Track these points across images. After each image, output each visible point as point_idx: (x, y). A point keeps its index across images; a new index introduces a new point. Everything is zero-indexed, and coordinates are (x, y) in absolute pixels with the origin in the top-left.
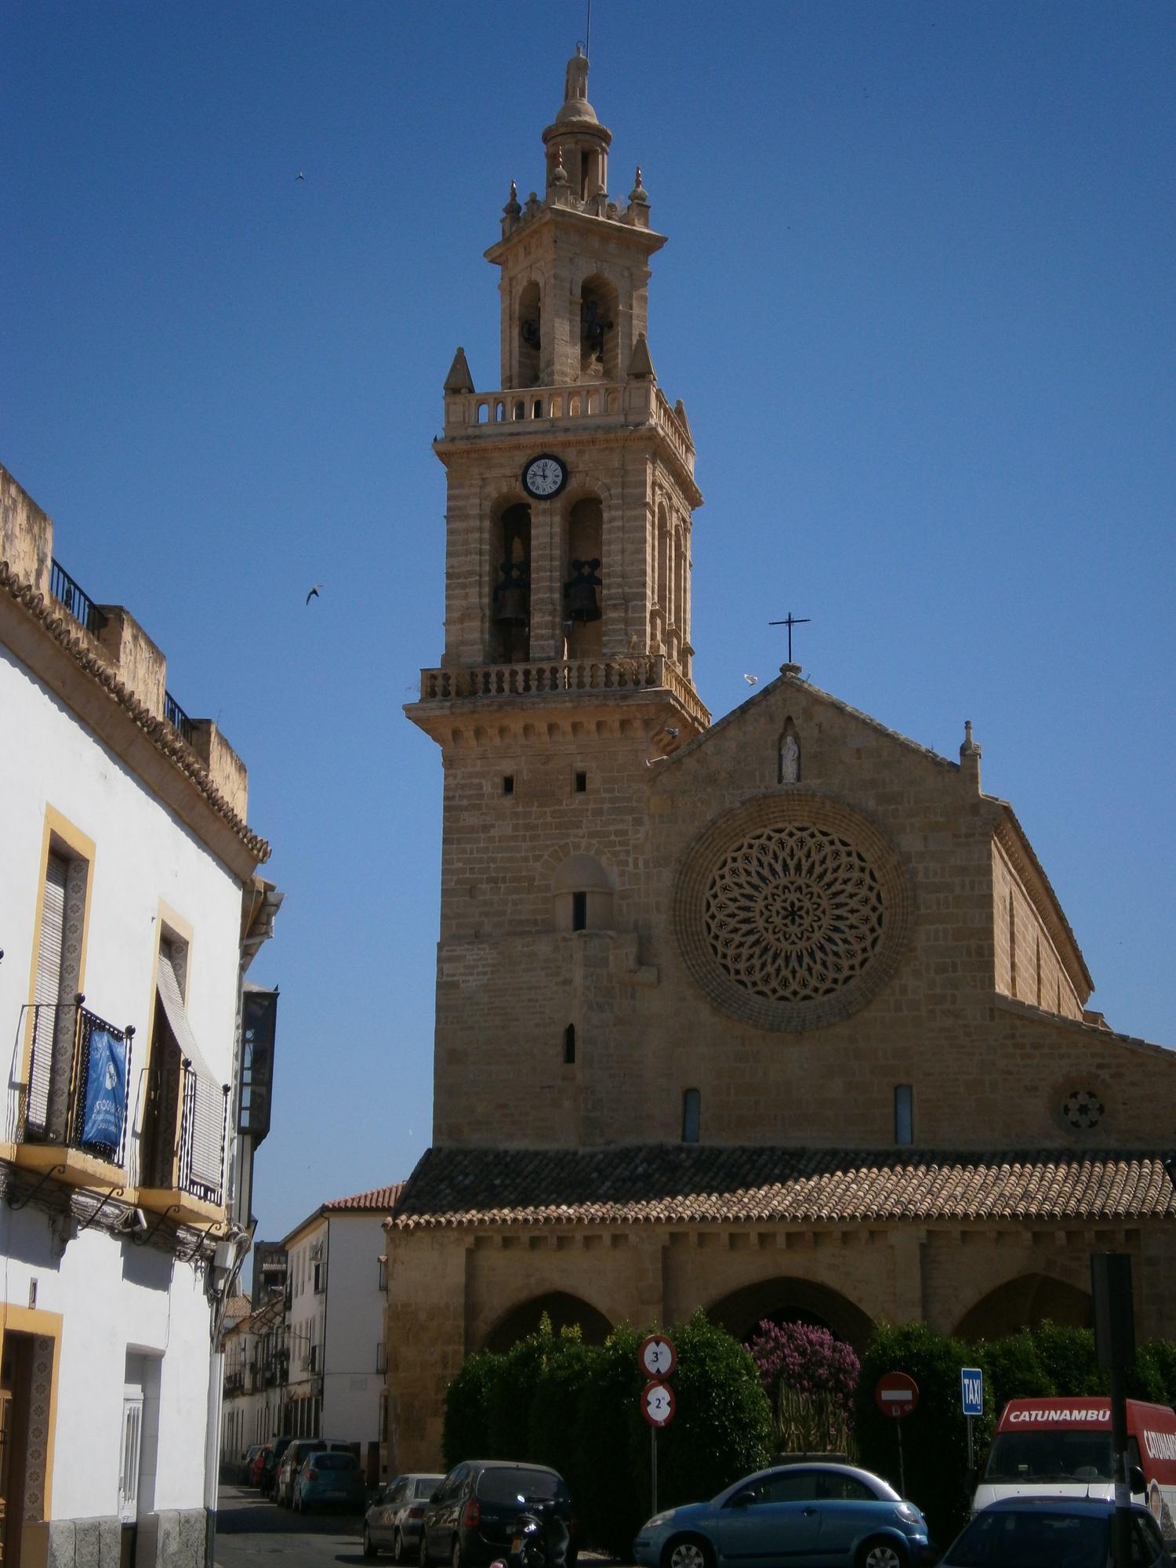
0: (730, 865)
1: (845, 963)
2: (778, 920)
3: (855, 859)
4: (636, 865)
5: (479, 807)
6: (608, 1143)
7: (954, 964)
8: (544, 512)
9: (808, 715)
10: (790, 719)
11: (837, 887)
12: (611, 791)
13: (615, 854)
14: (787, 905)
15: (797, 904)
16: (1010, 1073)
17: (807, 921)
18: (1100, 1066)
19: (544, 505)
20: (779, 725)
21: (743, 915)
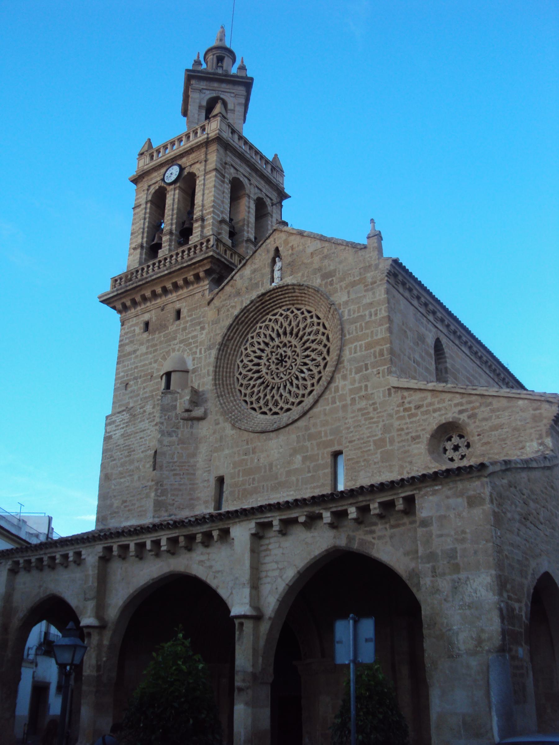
1: (309, 383)
2: (273, 367)
3: (315, 320)
5: (132, 342)
6: (170, 515)
8: (171, 190)
9: (286, 242)
10: (277, 250)
12: (191, 315)
13: (190, 350)
14: (278, 356)
16: (402, 429)
18: (461, 412)
20: (272, 254)
21: (255, 368)
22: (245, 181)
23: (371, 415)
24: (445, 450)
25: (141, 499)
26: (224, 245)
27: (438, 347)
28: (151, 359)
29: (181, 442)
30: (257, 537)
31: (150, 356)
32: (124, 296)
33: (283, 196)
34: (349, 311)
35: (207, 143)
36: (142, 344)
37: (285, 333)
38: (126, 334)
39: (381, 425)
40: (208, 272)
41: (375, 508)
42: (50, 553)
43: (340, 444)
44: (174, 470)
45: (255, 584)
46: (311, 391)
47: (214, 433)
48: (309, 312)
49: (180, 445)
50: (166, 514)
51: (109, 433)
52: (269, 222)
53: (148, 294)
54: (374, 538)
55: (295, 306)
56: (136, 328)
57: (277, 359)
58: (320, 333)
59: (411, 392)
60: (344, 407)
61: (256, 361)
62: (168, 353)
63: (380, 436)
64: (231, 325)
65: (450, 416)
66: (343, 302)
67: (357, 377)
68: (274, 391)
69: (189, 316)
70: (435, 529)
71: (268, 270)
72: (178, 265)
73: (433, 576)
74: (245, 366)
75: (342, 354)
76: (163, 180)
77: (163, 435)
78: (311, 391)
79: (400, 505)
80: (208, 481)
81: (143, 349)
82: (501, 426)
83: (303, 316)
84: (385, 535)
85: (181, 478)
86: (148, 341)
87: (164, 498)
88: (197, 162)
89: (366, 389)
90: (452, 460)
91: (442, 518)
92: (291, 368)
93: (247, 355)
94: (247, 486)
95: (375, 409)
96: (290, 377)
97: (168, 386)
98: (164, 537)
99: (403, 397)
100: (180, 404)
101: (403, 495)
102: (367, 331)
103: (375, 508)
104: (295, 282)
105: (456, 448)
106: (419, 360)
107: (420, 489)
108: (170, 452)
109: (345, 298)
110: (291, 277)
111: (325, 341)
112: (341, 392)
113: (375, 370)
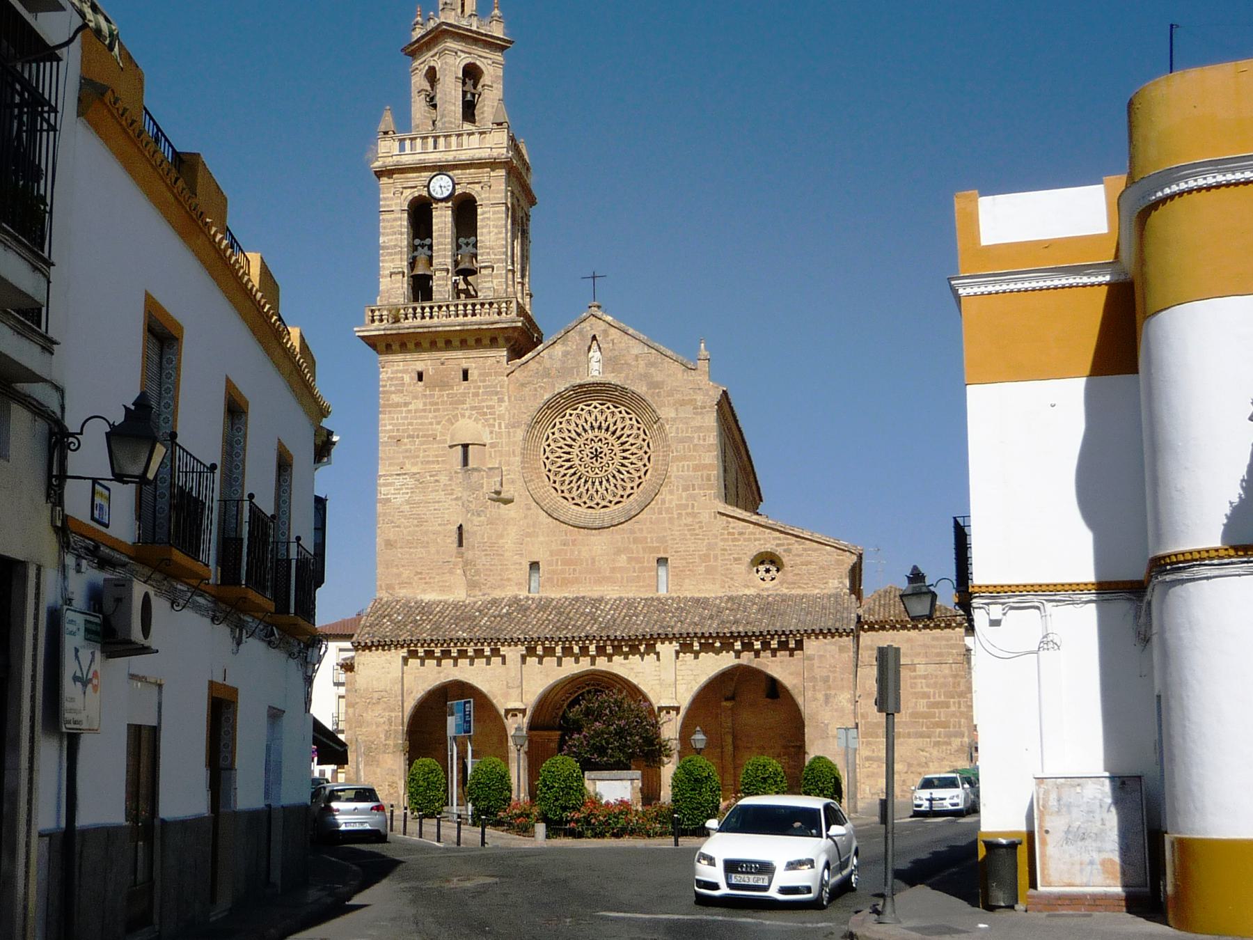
0: (558, 426)
1: (629, 485)
4: (500, 427)
9: (605, 332)
10: (594, 338)
11: (623, 439)
13: (486, 420)
17: (605, 461)
18: (778, 545)
19: (443, 204)
37: (600, 428)
43: (665, 552)
65: (769, 547)
70: (816, 662)
82: (810, 563)
91: (821, 656)
95: (701, 527)
105: (768, 571)
109: (673, 415)
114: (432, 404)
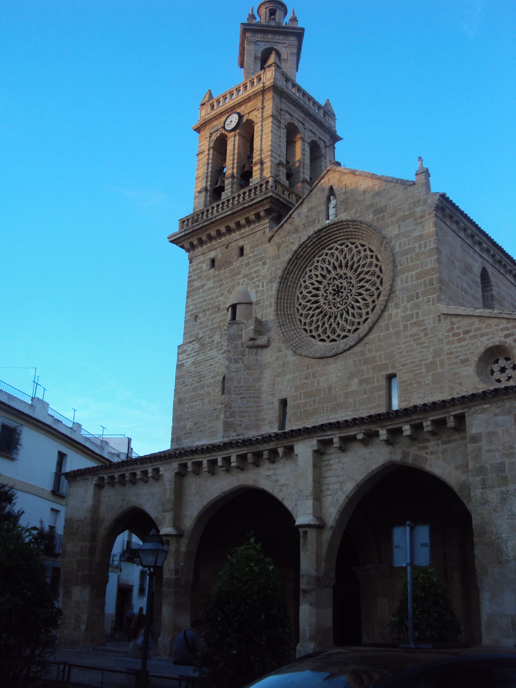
1: (364, 312)
2: (330, 297)
3: (368, 252)
4: (263, 286)
5: (200, 278)
6: (238, 435)
7: (417, 294)
10: (331, 188)
12: (254, 252)
15: (340, 285)
16: (452, 353)
18: (507, 336)
19: (233, 133)
20: (326, 193)
21: (313, 299)
22: (300, 126)
23: (423, 340)
24: (492, 372)
25: (213, 420)
26: (282, 185)
27: (484, 275)
28: (218, 292)
29: (247, 368)
30: (319, 453)
31: (217, 290)
32: (192, 236)
33: (335, 138)
34: (400, 244)
35: (263, 91)
36: (209, 279)
37: (341, 266)
38: (194, 270)
39: (432, 348)
40: (268, 212)
41: (427, 425)
42: (131, 470)
43: (393, 367)
44: (242, 394)
45: (318, 496)
46: (366, 319)
47: (277, 359)
48: (363, 246)
49: (247, 371)
50: (235, 434)
51: (181, 361)
52: (323, 163)
53: (213, 233)
54: (427, 453)
55: (350, 240)
56: (203, 265)
57: (334, 290)
58: (374, 264)
59: (460, 318)
60: (397, 334)
61: (314, 292)
62: (233, 287)
63: (431, 360)
64: (291, 259)
65: (496, 340)
66: (395, 235)
67: (409, 305)
68: (332, 320)
69: (251, 253)
70: (484, 445)
71: (323, 208)
72: (240, 206)
73: (483, 489)
74: (304, 297)
75: (394, 284)
76: (224, 127)
77: (230, 362)
78: (366, 319)
79: (451, 423)
80: (273, 403)
81: (210, 284)
83: (358, 249)
84: (437, 451)
85: (248, 401)
86: (215, 276)
87: (232, 419)
88: (255, 109)
89: (417, 316)
90: (499, 381)
92: (347, 298)
93: (306, 287)
94: (308, 408)
95: (426, 335)
96: (347, 307)
97: (234, 317)
98: (233, 455)
99: (452, 323)
100: (246, 333)
101: (454, 413)
102: (417, 262)
103: (428, 426)
104: (348, 218)
106: (467, 288)
107: (470, 408)
108: (237, 377)
109: (396, 232)
110: (345, 214)
111: (378, 272)
112: (394, 320)
113: (425, 298)
114: (219, 281)
